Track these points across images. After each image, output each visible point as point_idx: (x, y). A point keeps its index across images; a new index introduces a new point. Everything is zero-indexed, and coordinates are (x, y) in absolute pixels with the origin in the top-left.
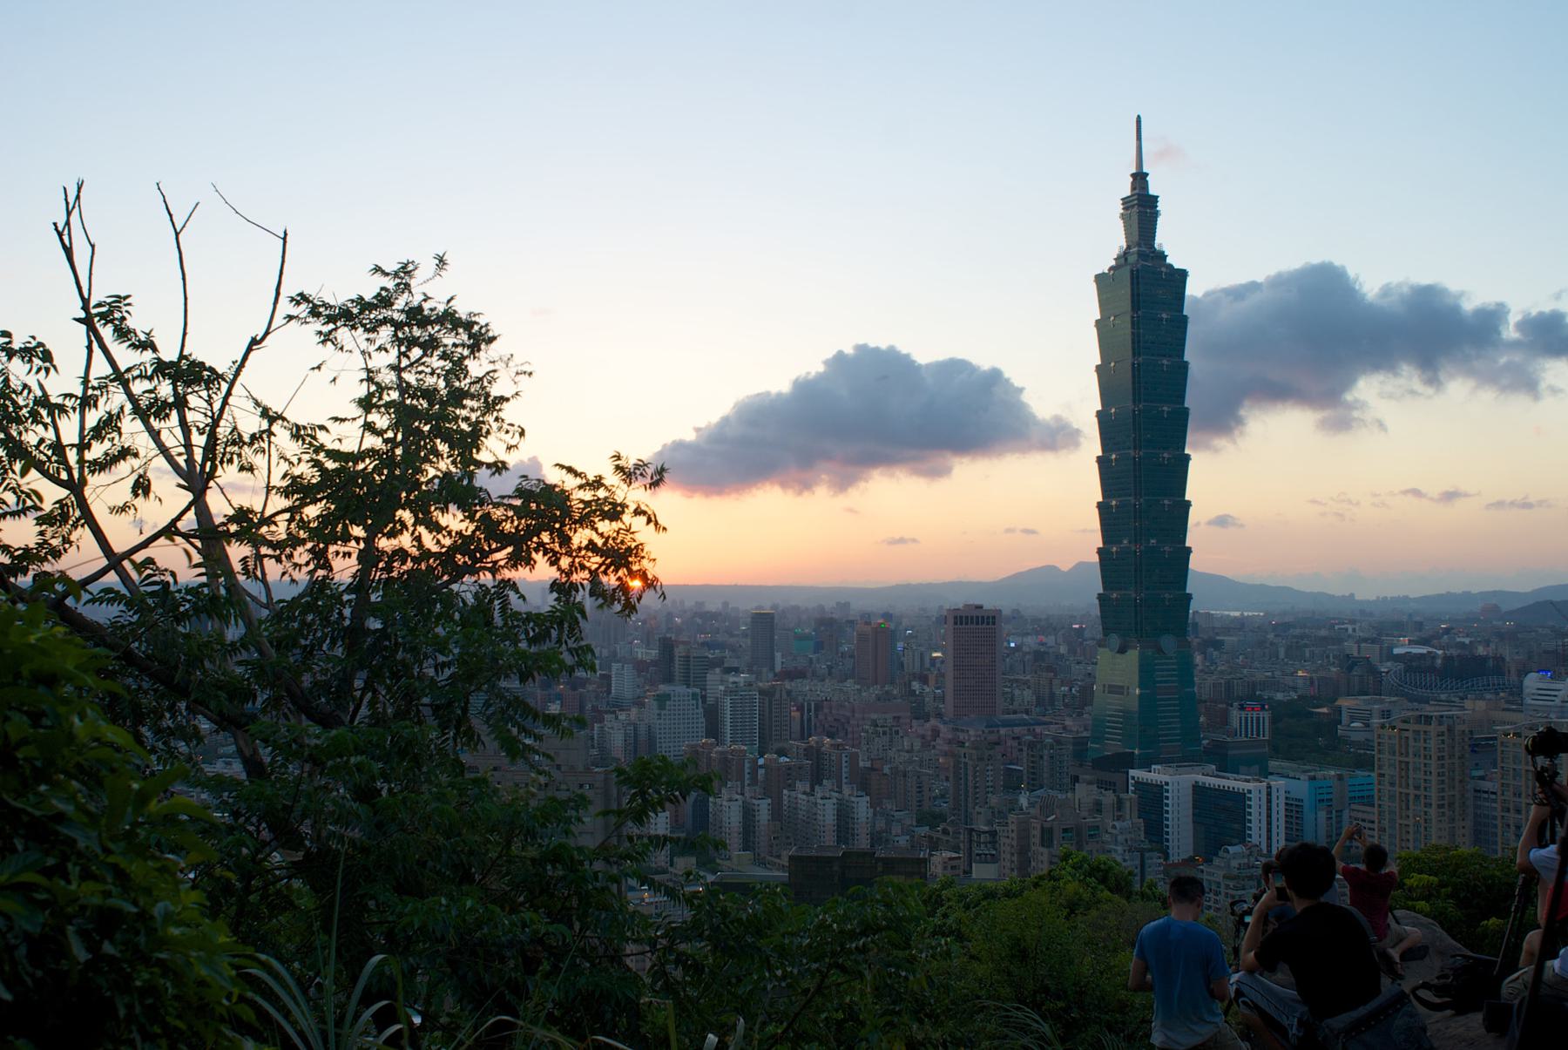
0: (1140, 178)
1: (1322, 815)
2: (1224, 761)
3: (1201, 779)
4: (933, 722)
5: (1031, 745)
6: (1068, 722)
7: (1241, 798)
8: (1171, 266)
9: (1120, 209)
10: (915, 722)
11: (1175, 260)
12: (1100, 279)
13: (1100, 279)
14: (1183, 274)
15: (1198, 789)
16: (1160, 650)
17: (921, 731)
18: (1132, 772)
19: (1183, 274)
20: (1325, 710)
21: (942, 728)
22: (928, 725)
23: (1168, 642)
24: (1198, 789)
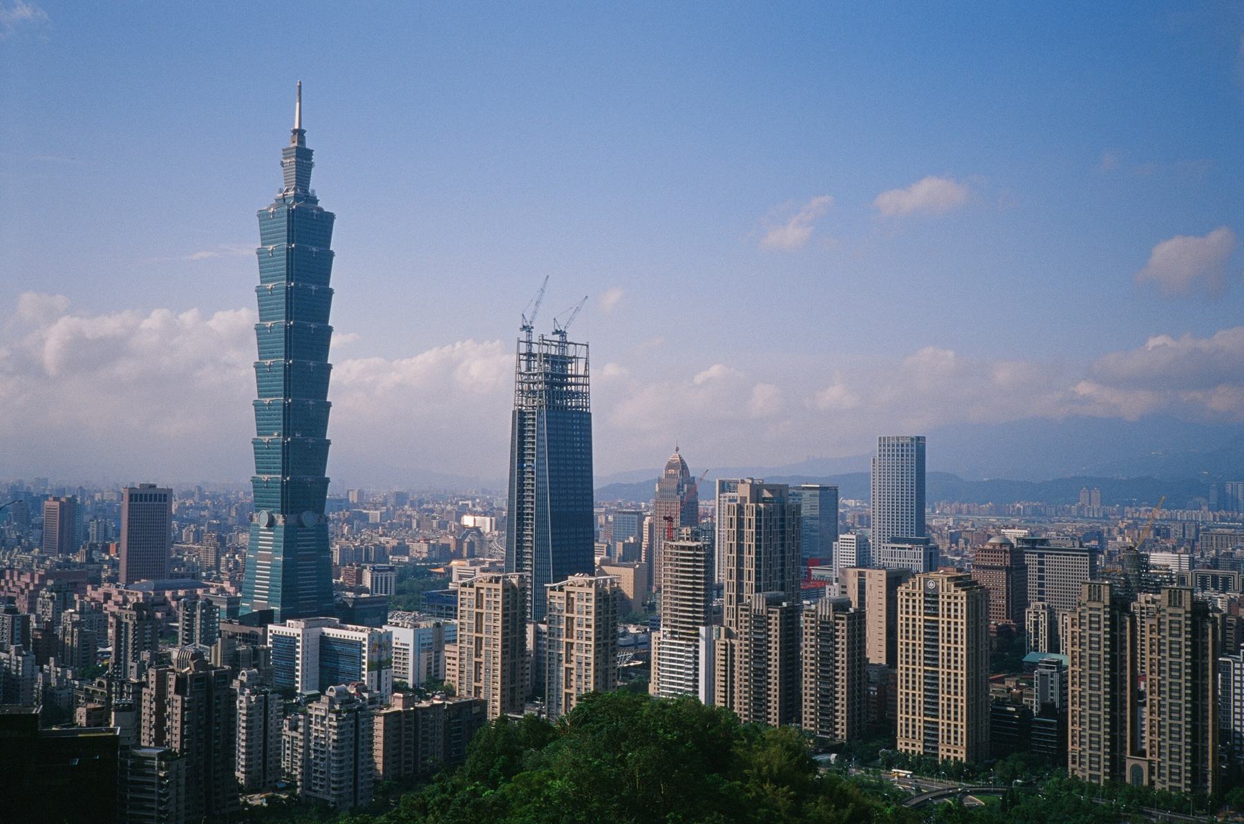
0: (300, 133)
2: (350, 616)
4: (106, 587)
6: (226, 585)
7: (359, 644)
8: (320, 209)
9: (280, 157)
11: (325, 204)
12: (263, 216)
13: (263, 216)
14: (330, 217)
17: (95, 595)
18: (270, 627)
19: (330, 217)
20: (441, 570)
21: (114, 592)
22: (101, 590)
23: (308, 518)
24: (324, 639)
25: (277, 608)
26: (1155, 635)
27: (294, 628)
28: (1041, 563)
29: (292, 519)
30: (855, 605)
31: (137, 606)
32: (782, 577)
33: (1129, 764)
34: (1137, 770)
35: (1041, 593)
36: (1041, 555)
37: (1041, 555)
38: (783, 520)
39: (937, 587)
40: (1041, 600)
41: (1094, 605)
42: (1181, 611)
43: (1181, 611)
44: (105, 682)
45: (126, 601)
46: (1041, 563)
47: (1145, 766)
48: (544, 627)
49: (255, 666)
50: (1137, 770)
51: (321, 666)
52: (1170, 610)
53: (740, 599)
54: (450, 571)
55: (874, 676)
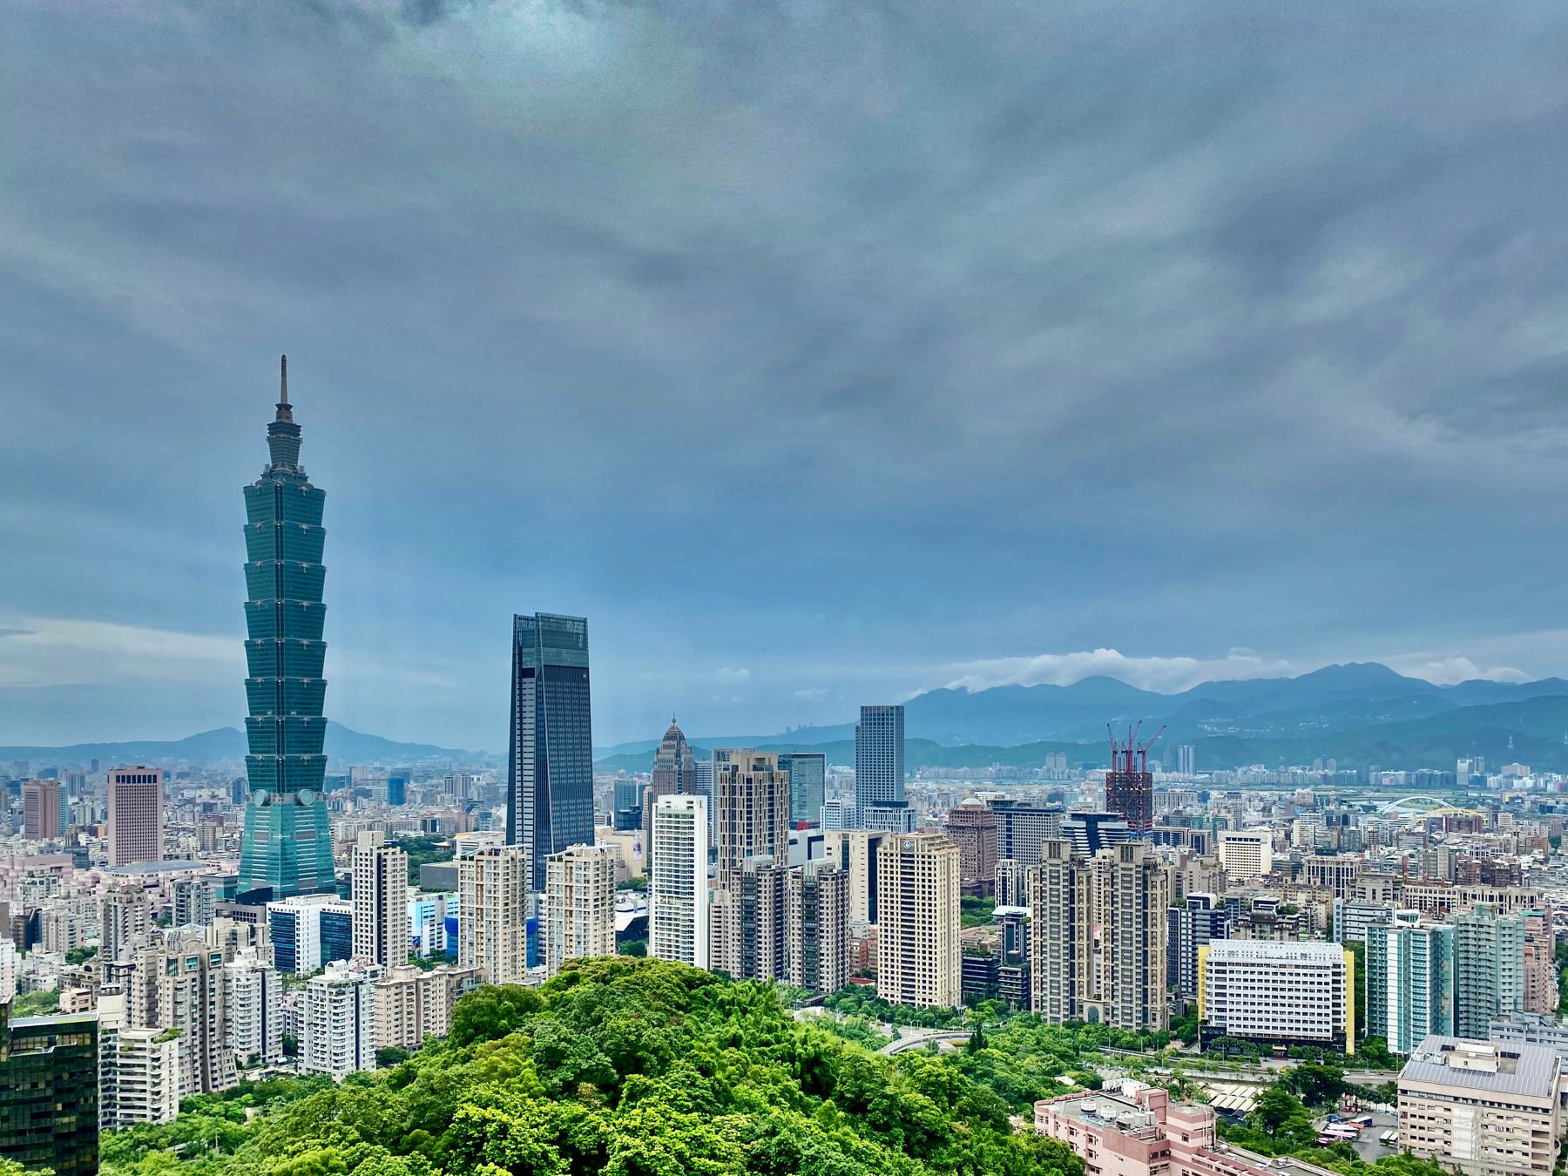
1: (427, 928)
3: (327, 907)
4: (95, 870)
5: (180, 888)
6: (223, 864)
10: (76, 872)
15: (325, 916)
16: (300, 803)
17: (81, 879)
18: (269, 904)
21: (103, 875)
22: (88, 874)
23: (306, 795)
25: (277, 886)
26: (1108, 888)
27: (290, 905)
28: (1009, 823)
29: (289, 798)
30: (839, 867)
31: (127, 890)
32: (771, 841)
33: (1086, 1007)
34: (1093, 1012)
35: (1009, 850)
36: (1009, 816)
37: (1009, 816)
38: (771, 787)
39: (912, 849)
40: (1009, 857)
41: (1055, 861)
42: (1132, 866)
43: (1132, 866)
44: (93, 967)
45: (116, 884)
46: (1009, 823)
47: (1100, 1008)
48: (543, 897)
49: (253, 944)
50: (1093, 1012)
51: (323, 941)
52: (1122, 865)
53: (733, 862)
54: (454, 844)
55: (857, 933)
